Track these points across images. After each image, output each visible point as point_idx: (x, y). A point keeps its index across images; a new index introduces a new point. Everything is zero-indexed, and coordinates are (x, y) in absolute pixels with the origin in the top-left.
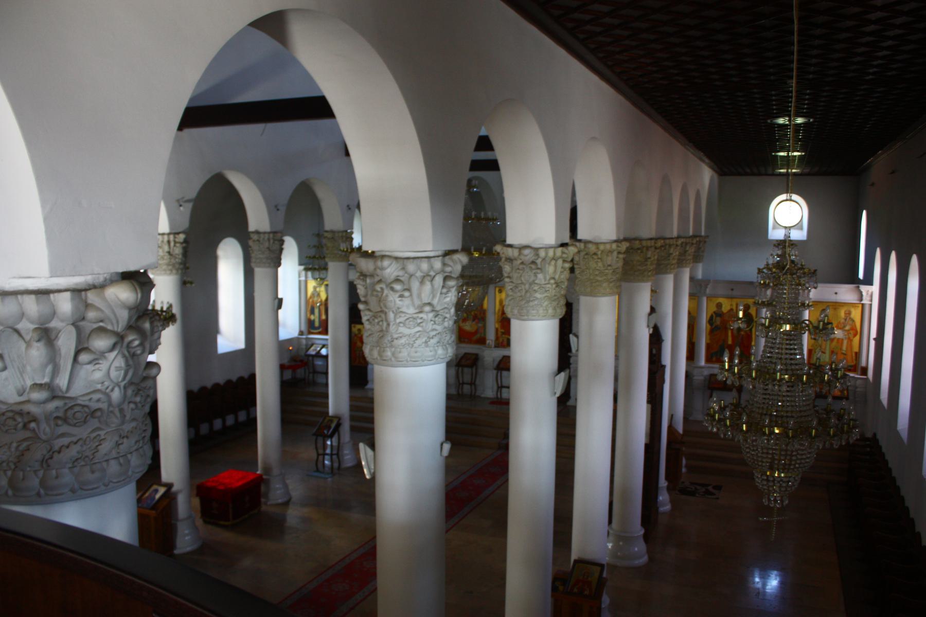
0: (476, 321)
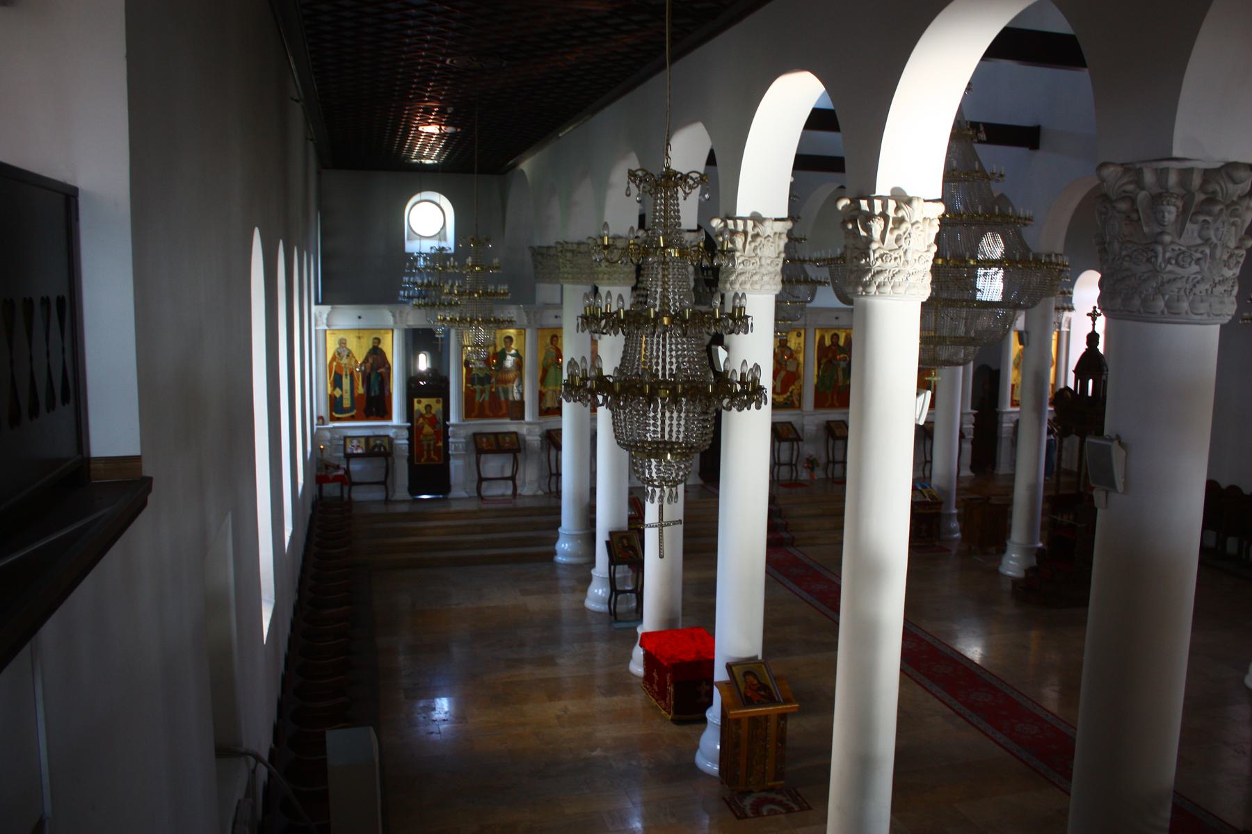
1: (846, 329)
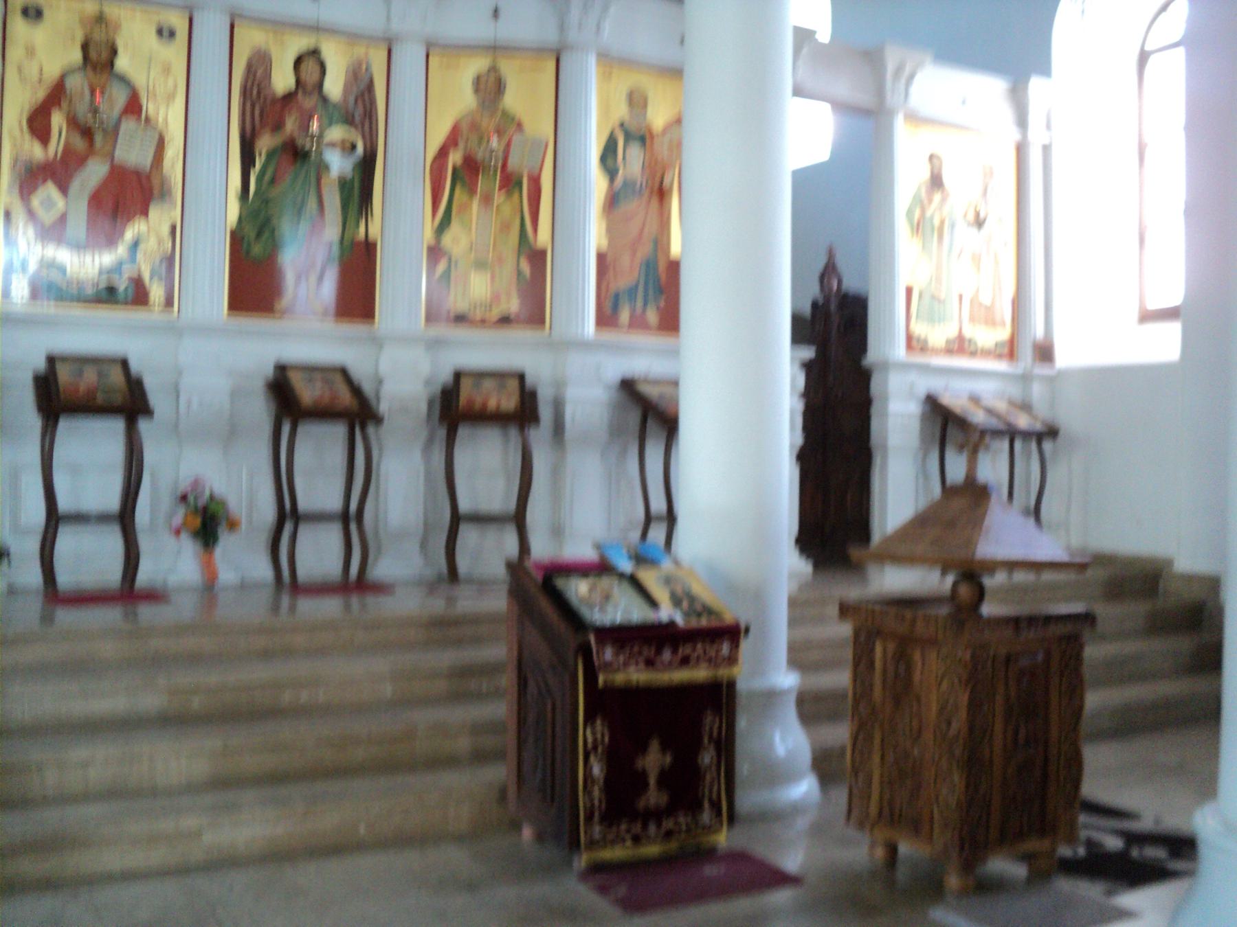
1: (352, 37)
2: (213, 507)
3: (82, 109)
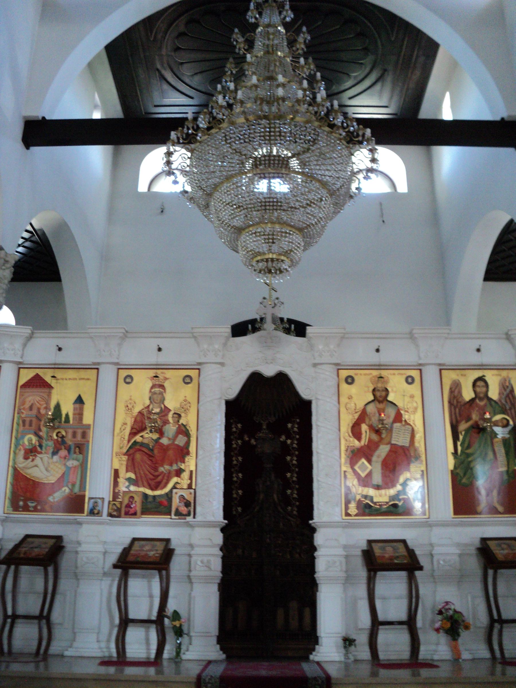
0: (63, 452)
1: (499, 368)
2: (456, 616)
3: (374, 420)
